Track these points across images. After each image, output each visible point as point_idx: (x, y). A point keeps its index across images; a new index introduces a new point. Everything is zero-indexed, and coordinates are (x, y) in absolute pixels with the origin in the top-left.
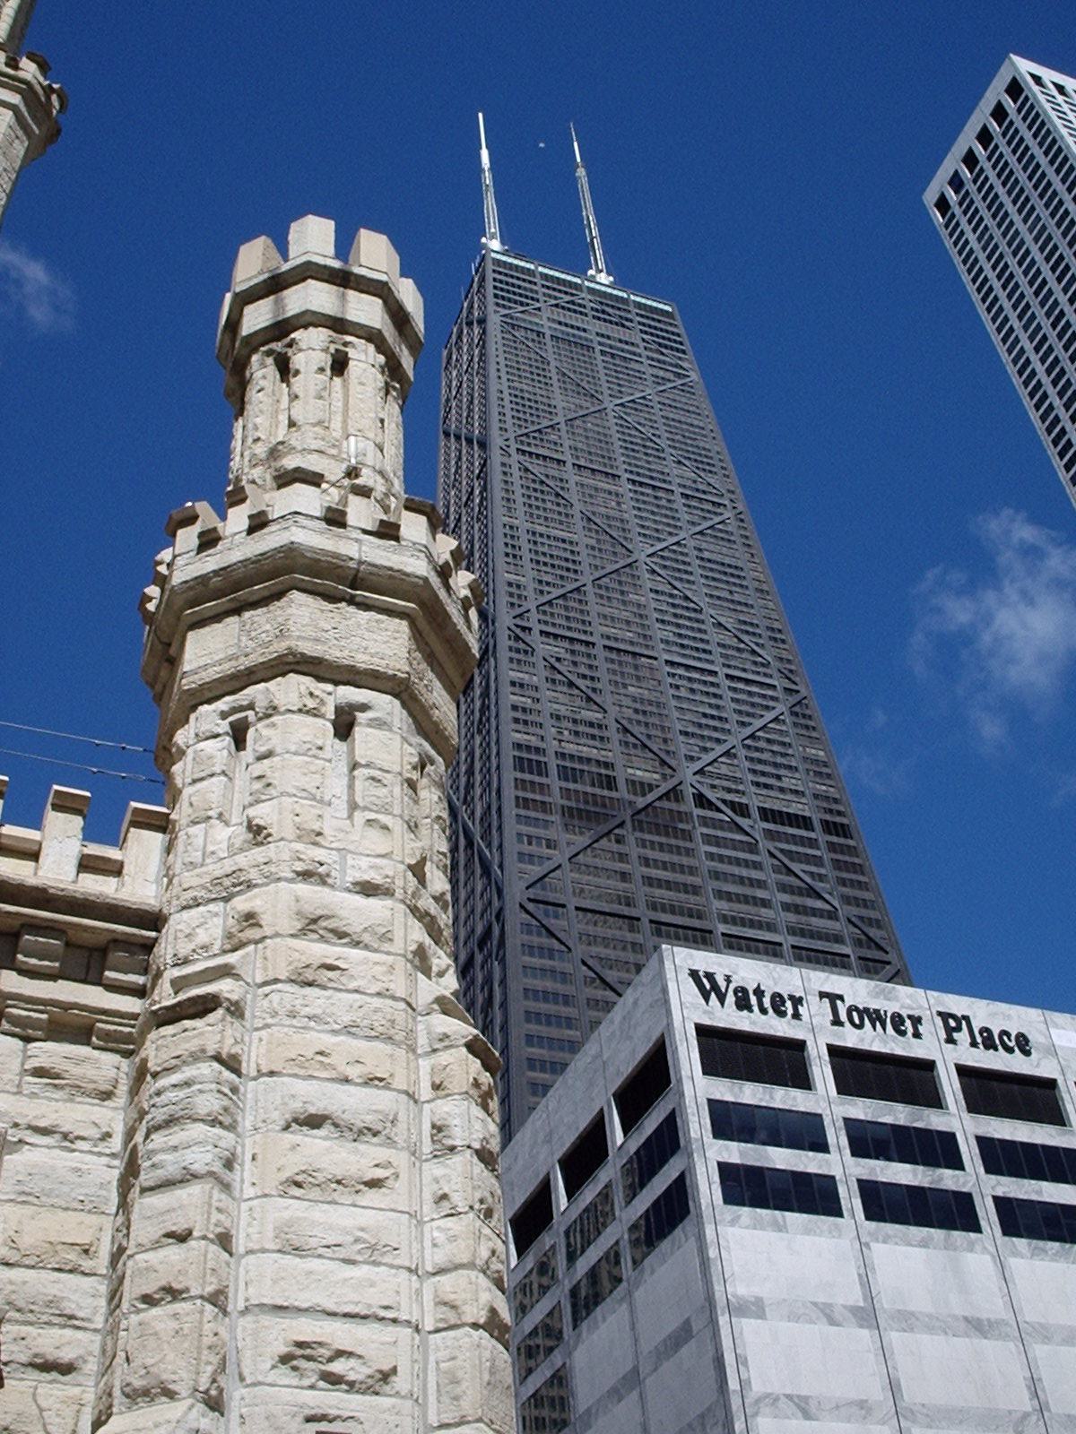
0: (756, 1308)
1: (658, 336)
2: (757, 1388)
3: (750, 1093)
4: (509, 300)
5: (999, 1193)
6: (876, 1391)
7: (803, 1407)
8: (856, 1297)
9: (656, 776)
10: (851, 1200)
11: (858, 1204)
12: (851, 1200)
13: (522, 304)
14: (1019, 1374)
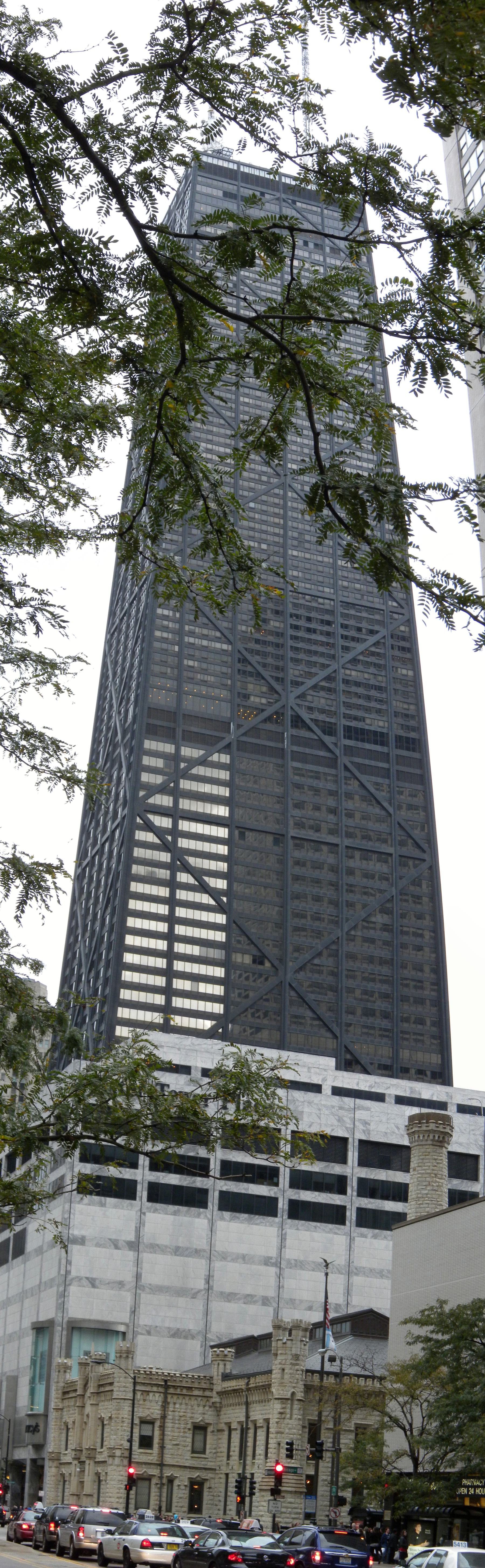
0: (81, 1241)
2: (74, 1273)
5: (224, 1189)
6: (128, 1277)
7: (93, 1283)
8: (131, 1237)
9: (264, 701)
10: (142, 1192)
11: (145, 1194)
12: (142, 1192)
14: (203, 1273)
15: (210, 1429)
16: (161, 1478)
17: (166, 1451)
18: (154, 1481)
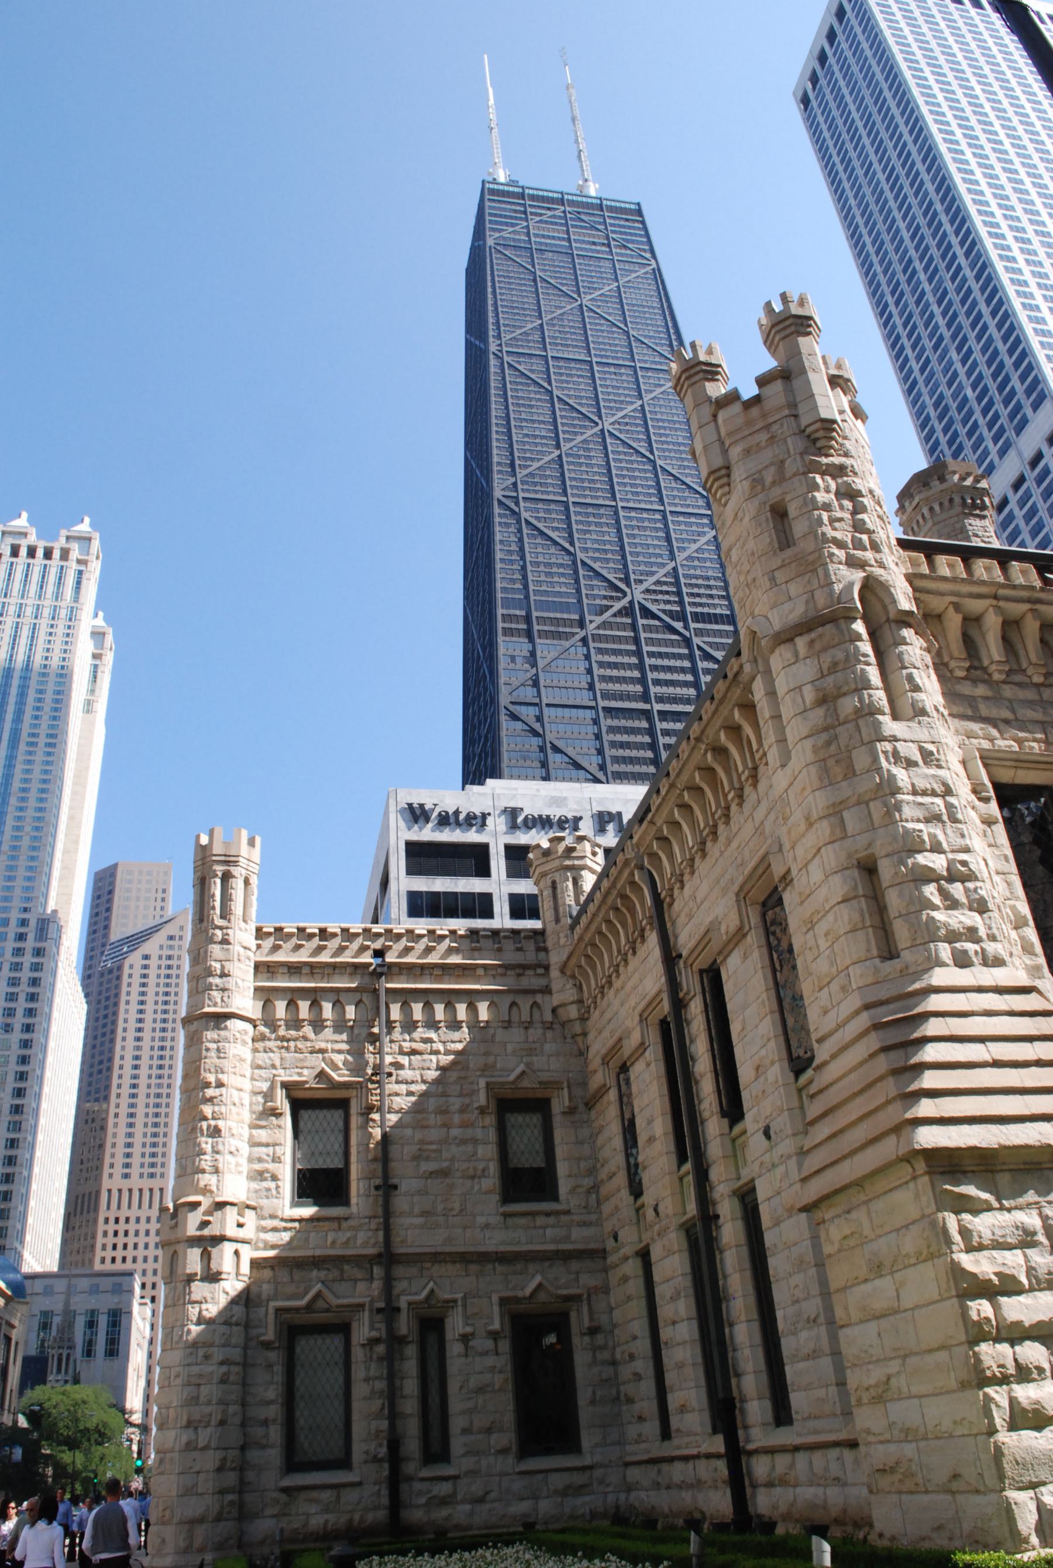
1: (626, 233)
3: (441, 884)
4: (501, 223)
15: (558, 1106)
16: (389, 1311)
17: (400, 1202)
18: (363, 1330)
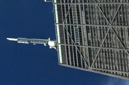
4: (79, 60)
13: (79, 55)
